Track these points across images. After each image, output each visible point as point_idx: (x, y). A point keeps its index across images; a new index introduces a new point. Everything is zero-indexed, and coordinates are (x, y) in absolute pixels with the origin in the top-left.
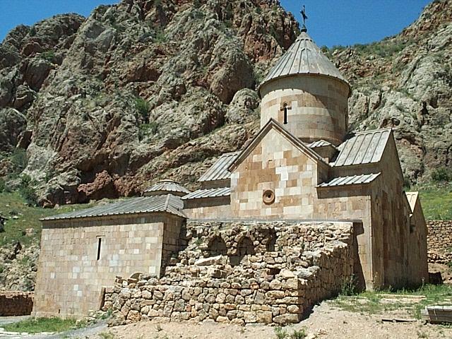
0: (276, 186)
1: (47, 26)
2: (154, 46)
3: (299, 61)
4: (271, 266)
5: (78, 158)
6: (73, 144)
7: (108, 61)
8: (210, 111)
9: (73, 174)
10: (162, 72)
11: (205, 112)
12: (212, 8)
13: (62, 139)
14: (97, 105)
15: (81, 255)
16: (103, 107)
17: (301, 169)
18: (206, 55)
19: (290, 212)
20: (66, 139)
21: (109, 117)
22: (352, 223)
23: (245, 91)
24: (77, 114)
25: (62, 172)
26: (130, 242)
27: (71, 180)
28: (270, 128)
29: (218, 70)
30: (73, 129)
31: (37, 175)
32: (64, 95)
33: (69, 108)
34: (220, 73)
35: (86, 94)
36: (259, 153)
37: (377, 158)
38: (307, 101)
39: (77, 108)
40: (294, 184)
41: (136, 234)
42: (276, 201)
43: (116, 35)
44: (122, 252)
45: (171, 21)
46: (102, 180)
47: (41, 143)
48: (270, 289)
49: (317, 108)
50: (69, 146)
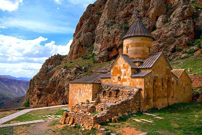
0: (121, 75)
1: (98, 3)
4: (101, 107)
6: (105, 42)
7: (116, 12)
8: (149, 26)
9: (106, 52)
13: (102, 41)
15: (77, 93)
17: (127, 70)
19: (125, 84)
21: (115, 32)
22: (138, 89)
25: (103, 51)
26: (86, 90)
27: (105, 54)
29: (152, 9)
31: (96, 52)
33: (104, 30)
34: (152, 11)
37: (150, 67)
40: (125, 75)
41: (87, 88)
42: (121, 80)
44: (84, 93)
47: (97, 42)
48: (89, 118)
49: (137, 47)
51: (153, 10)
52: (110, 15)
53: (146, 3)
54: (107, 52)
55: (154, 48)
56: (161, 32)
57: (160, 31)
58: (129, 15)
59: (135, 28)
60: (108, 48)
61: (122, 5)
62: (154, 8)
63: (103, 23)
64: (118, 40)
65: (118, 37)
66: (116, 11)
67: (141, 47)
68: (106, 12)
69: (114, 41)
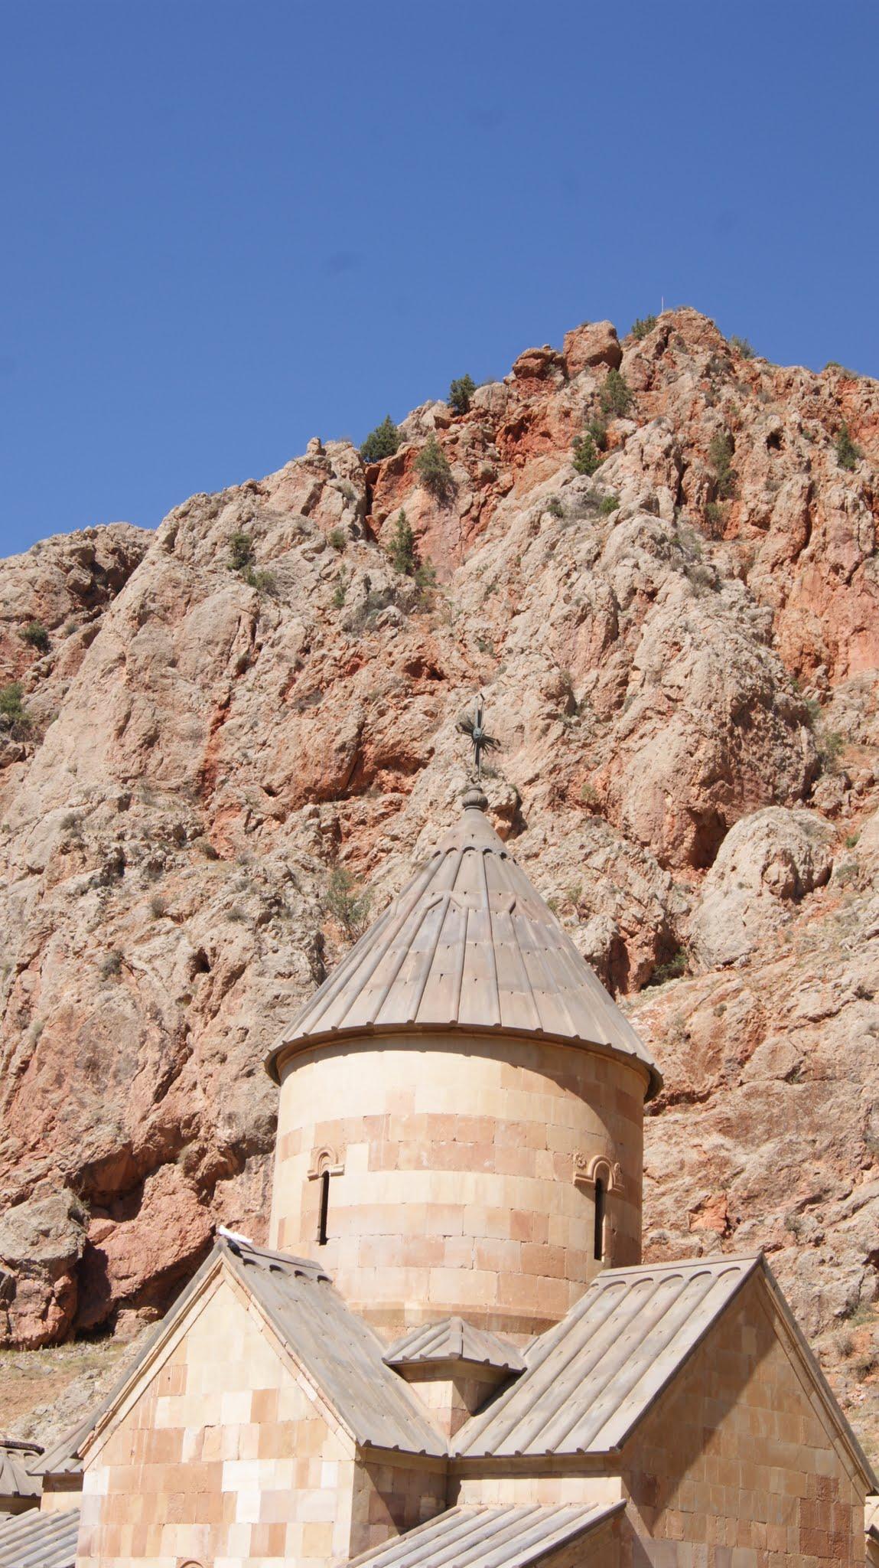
2: (405, 646)
3: (400, 952)
5: (76, 1141)
6: (59, 1080)
7: (221, 721)
10: (431, 752)
11: (595, 920)
12: (646, 467)
13: (16, 1061)
14: (159, 914)
16: (178, 919)
18: (609, 674)
20: (34, 1063)
21: (201, 963)
23: (764, 821)
24: (78, 954)
28: (218, 1272)
30: (62, 1018)
32: (40, 871)
33: (52, 929)
35: (120, 865)
36: (176, 1388)
37: (607, 1440)
38: (407, 1144)
39: (83, 925)
43: (257, 615)
45: (483, 530)
46: (172, 1231)
49: (449, 1175)
50: (47, 1091)
51: (661, 736)
52: (151, 741)
53: (580, 660)
54: (73, 1215)
55: (668, 1201)
56: (758, 1009)
57: (738, 991)
58: (374, 774)
59: (428, 931)
60: (89, 1170)
61: (306, 650)
62: (676, 722)
63: (58, 837)
64: (232, 1068)
65: (231, 1021)
66: (225, 706)
67: (491, 1170)
68: (107, 714)
69: (171, 1076)
